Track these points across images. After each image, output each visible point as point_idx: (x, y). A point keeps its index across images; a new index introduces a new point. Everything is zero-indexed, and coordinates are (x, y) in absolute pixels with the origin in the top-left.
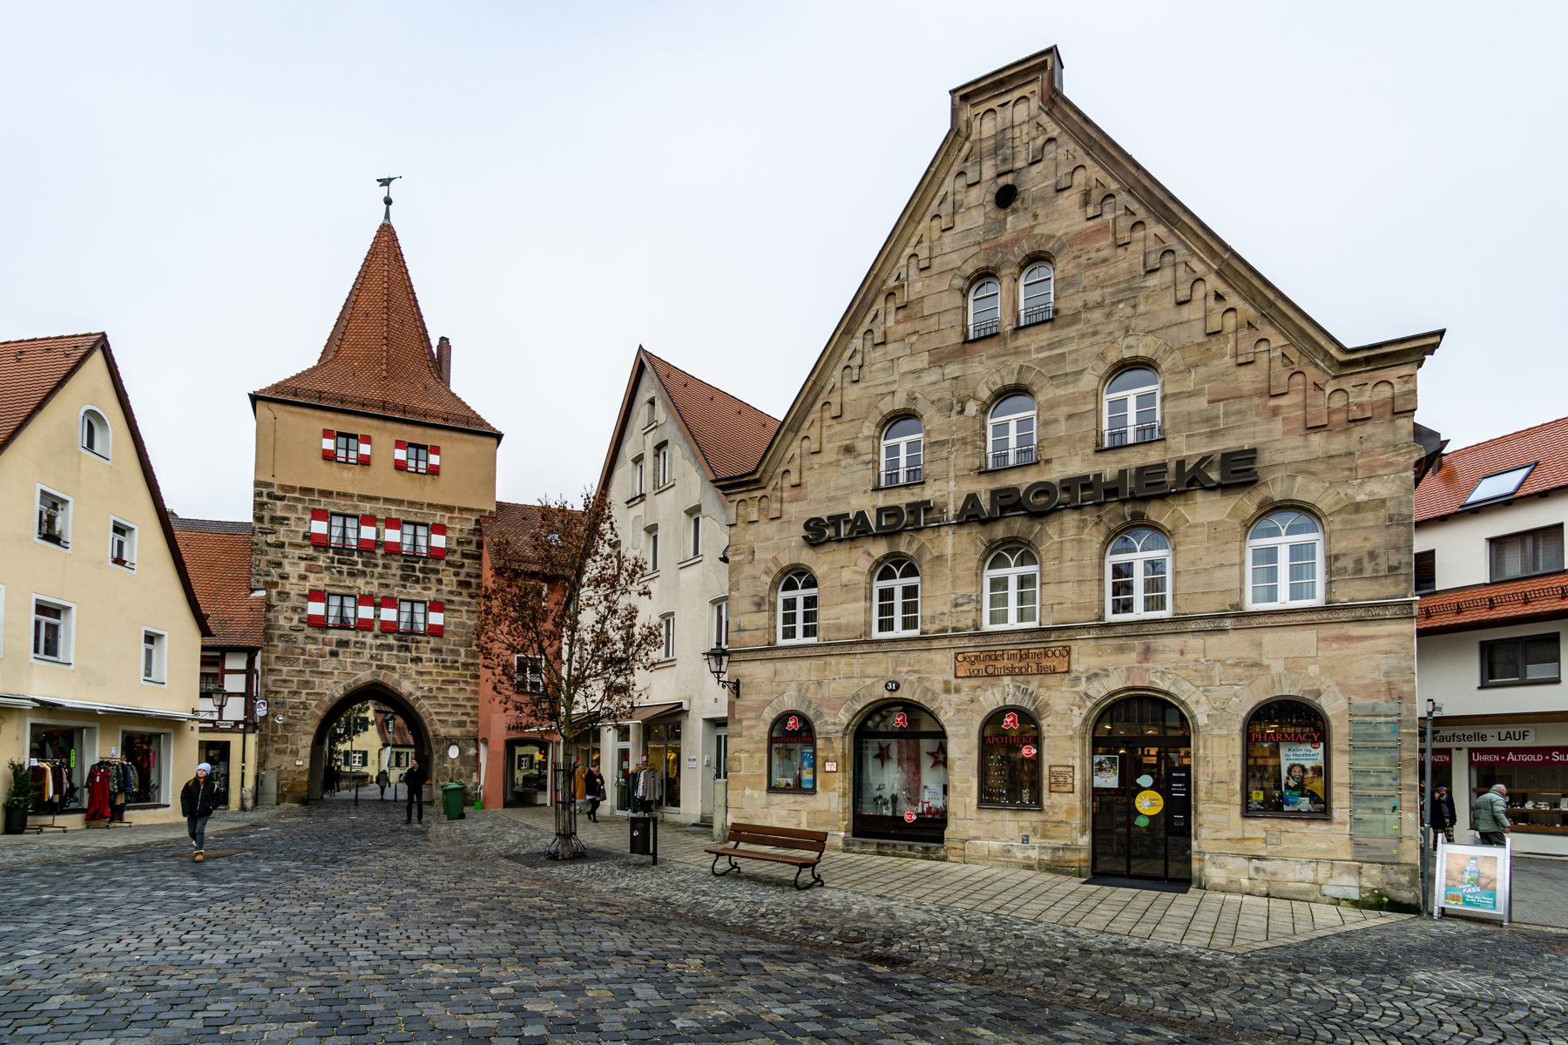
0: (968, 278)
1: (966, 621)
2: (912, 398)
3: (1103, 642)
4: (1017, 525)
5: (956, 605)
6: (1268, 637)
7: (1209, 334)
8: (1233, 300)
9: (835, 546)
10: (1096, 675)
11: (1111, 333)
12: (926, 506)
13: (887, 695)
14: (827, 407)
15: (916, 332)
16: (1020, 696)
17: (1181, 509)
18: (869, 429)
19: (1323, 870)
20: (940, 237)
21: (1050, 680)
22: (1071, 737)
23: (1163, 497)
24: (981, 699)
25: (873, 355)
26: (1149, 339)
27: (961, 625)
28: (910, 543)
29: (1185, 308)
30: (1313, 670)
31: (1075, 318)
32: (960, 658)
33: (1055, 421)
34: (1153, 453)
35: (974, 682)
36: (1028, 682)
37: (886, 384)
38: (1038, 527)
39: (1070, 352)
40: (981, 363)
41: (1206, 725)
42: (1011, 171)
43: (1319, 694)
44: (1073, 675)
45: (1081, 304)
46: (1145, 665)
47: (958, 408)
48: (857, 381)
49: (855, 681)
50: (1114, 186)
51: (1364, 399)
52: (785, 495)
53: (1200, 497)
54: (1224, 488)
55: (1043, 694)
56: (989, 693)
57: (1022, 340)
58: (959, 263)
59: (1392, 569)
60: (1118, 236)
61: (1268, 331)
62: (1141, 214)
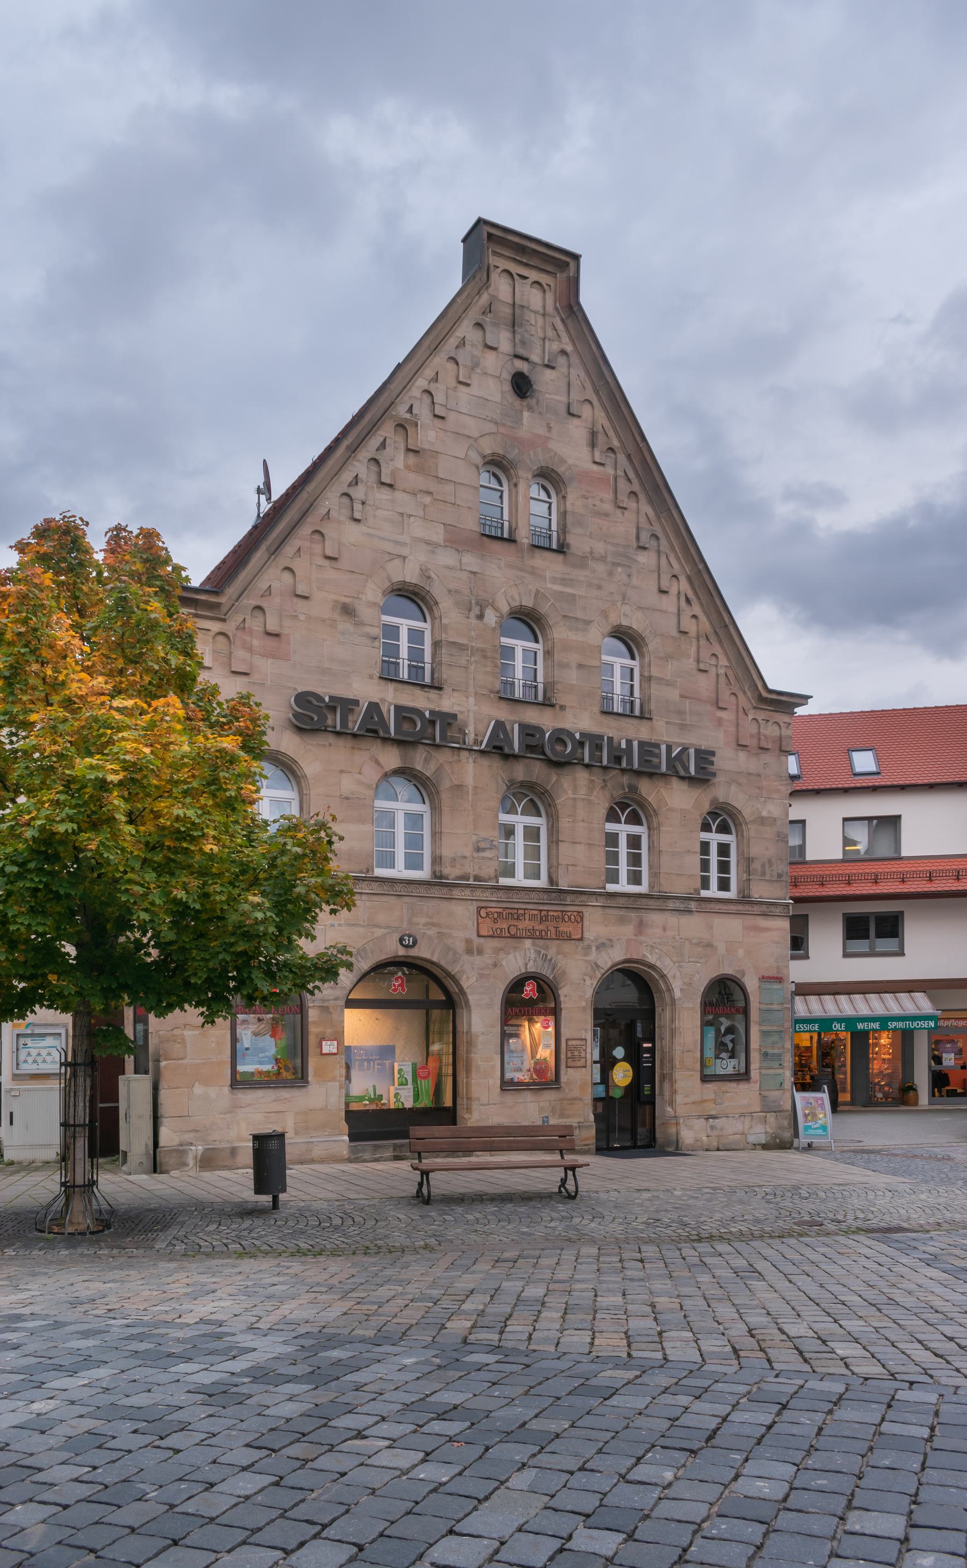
0: (484, 457)
1: (488, 870)
2: (425, 573)
3: (609, 911)
4: (536, 771)
5: (478, 849)
6: (719, 923)
7: (681, 632)
8: (697, 609)
9: (331, 739)
10: (603, 944)
11: (612, 593)
12: (448, 720)
13: (402, 952)
14: (317, 537)
15: (430, 493)
16: (540, 962)
17: (662, 791)
18: (373, 593)
19: (747, 1120)
20: (456, 387)
21: (567, 947)
22: (584, 1009)
23: (651, 775)
24: (504, 963)
25: (378, 496)
26: (639, 614)
27: (483, 874)
28: (427, 761)
29: (664, 597)
30: (741, 953)
31: (582, 562)
32: (483, 913)
33: (566, 666)
34: (643, 729)
35: (496, 943)
36: (547, 948)
37: (396, 542)
38: (554, 778)
39: (580, 597)
40: (500, 568)
41: (680, 999)
42: (526, 359)
43: (744, 975)
44: (586, 943)
45: (588, 550)
46: (642, 938)
47: (476, 610)
48: (358, 521)
49: (362, 930)
50: (616, 443)
51: (767, 732)
52: (256, 643)
53: (675, 783)
54: (690, 780)
55: (562, 962)
56: (511, 956)
57: (542, 561)
58: (475, 434)
59: (780, 876)
60: (620, 497)
61: (718, 650)
62: (636, 487)
